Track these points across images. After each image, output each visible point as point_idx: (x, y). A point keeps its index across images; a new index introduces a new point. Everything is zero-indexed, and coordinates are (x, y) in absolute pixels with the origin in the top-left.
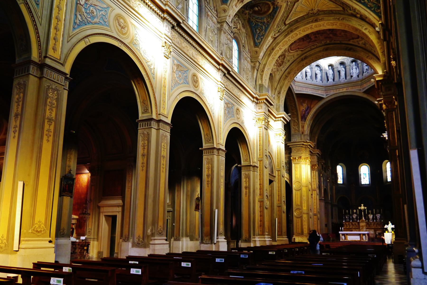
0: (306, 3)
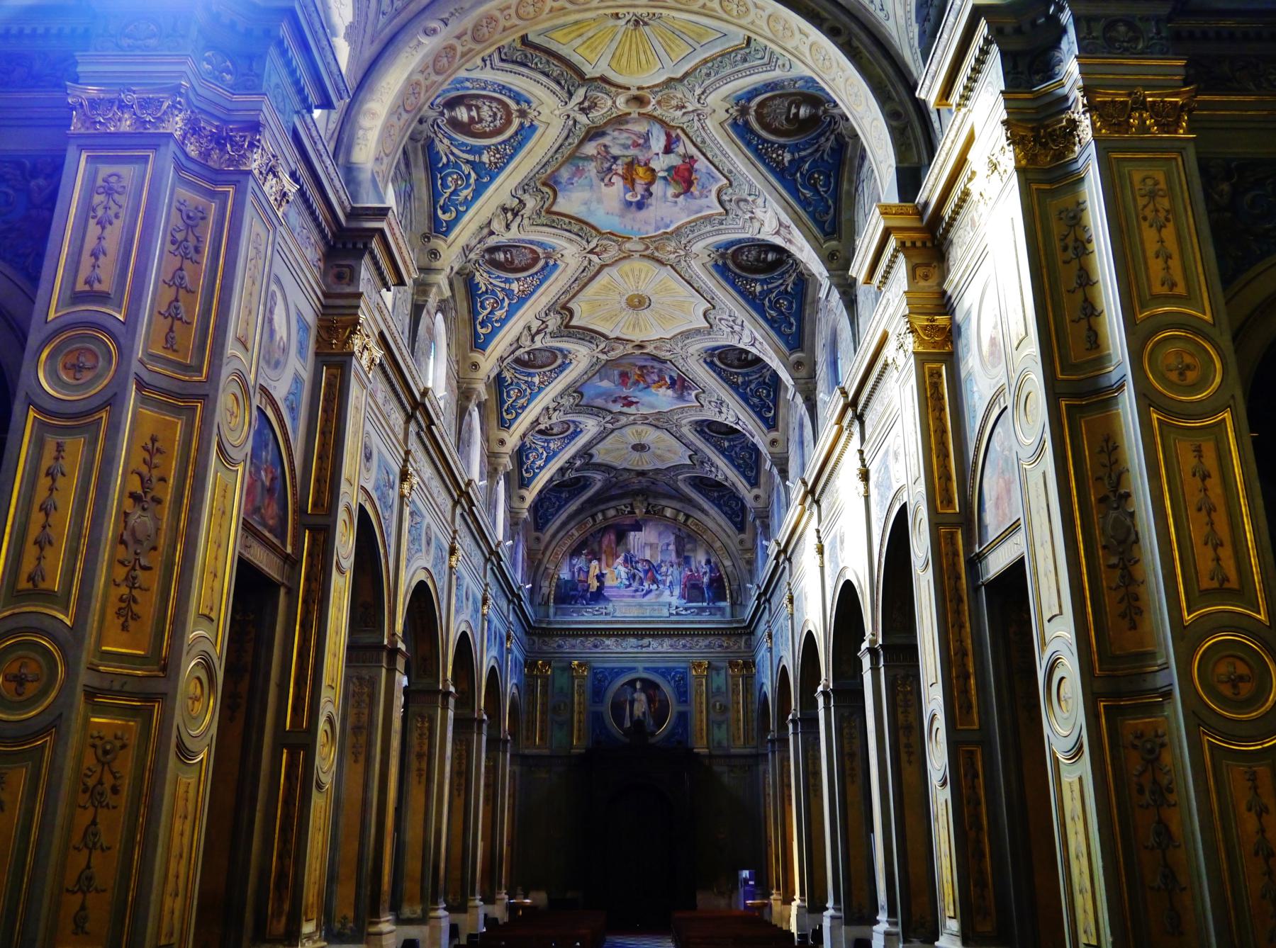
0: (648, 62)
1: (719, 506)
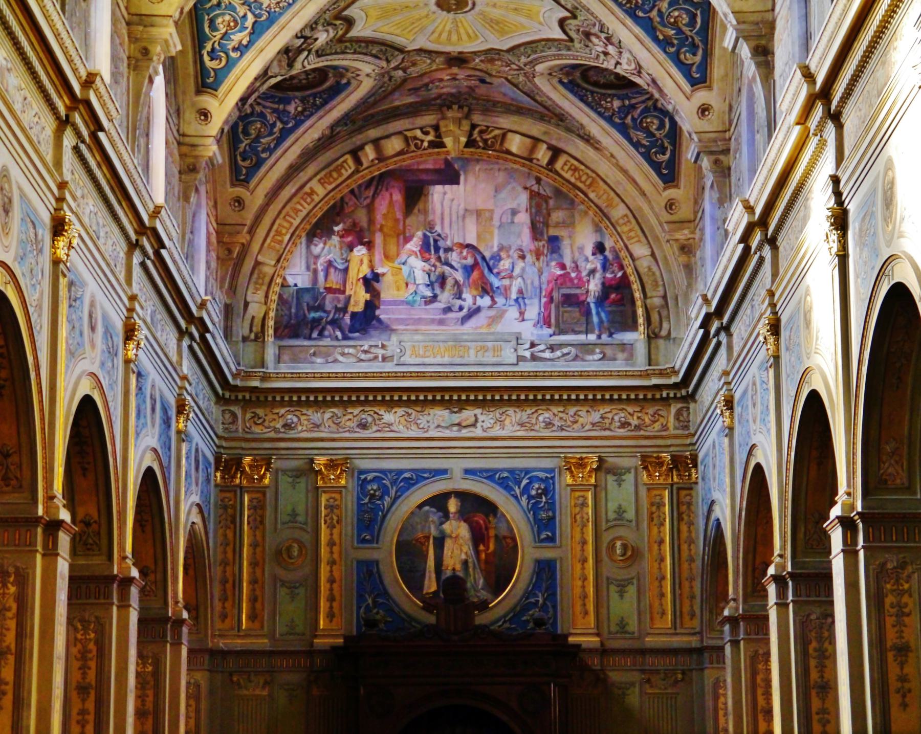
1: (623, 130)
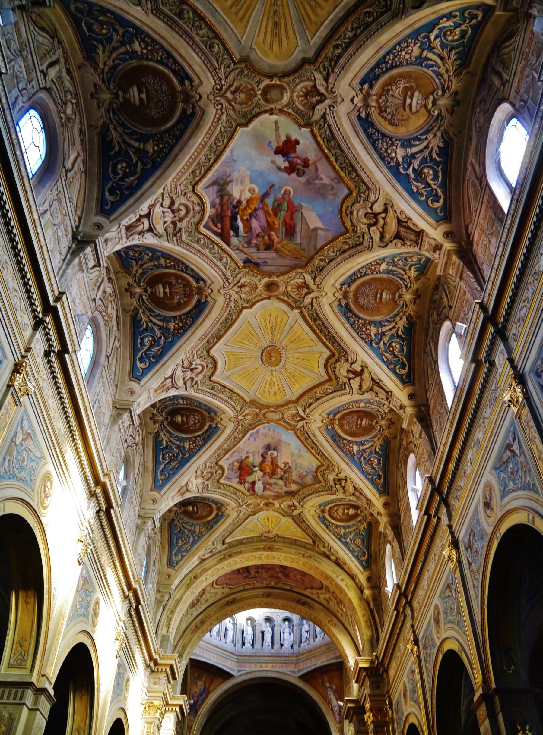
0: (264, 520)
